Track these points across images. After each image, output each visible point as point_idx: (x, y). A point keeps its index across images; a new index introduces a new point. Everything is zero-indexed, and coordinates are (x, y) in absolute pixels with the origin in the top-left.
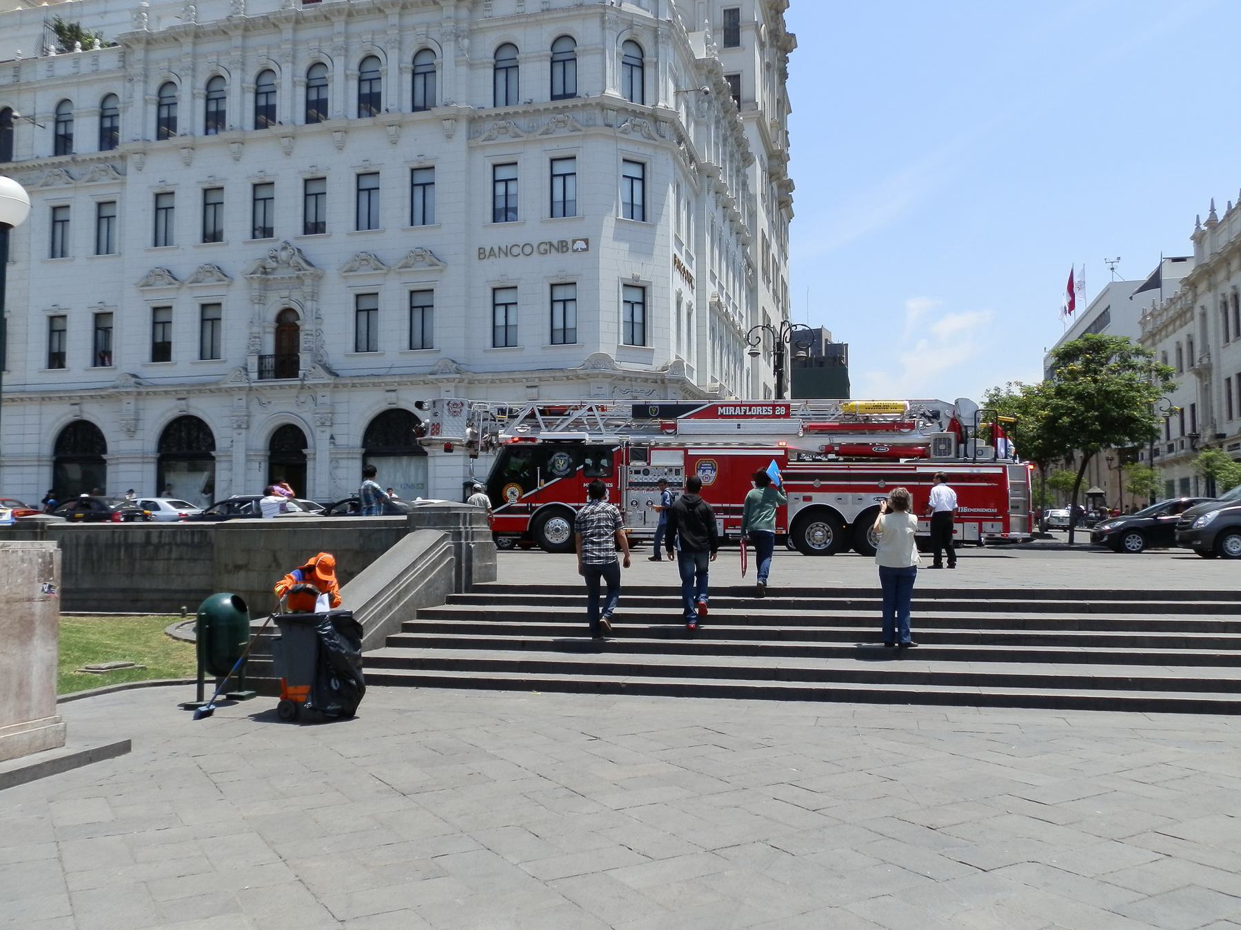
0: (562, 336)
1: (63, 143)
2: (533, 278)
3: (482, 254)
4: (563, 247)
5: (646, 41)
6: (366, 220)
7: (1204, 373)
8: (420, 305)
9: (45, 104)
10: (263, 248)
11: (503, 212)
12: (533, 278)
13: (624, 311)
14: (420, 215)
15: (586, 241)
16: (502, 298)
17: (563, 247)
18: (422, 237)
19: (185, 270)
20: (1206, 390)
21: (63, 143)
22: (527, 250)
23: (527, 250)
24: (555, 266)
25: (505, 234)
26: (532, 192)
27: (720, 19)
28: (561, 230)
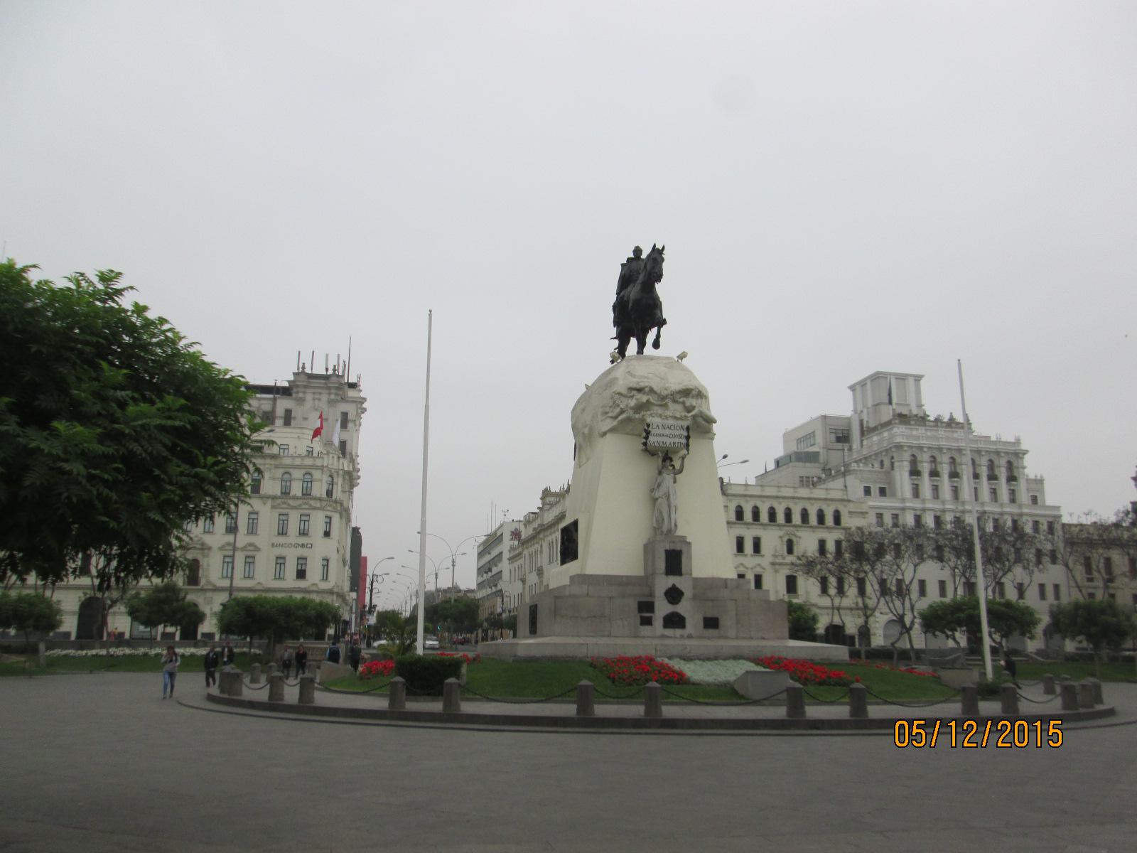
0: (301, 574)
3: (273, 545)
4: (303, 546)
5: (335, 474)
7: (523, 581)
8: (250, 561)
11: (282, 533)
13: (321, 568)
14: (252, 530)
15: (312, 545)
16: (280, 561)
17: (303, 546)
18: (252, 539)
20: (524, 588)
22: (290, 545)
23: (290, 545)
25: (282, 540)
26: (293, 526)
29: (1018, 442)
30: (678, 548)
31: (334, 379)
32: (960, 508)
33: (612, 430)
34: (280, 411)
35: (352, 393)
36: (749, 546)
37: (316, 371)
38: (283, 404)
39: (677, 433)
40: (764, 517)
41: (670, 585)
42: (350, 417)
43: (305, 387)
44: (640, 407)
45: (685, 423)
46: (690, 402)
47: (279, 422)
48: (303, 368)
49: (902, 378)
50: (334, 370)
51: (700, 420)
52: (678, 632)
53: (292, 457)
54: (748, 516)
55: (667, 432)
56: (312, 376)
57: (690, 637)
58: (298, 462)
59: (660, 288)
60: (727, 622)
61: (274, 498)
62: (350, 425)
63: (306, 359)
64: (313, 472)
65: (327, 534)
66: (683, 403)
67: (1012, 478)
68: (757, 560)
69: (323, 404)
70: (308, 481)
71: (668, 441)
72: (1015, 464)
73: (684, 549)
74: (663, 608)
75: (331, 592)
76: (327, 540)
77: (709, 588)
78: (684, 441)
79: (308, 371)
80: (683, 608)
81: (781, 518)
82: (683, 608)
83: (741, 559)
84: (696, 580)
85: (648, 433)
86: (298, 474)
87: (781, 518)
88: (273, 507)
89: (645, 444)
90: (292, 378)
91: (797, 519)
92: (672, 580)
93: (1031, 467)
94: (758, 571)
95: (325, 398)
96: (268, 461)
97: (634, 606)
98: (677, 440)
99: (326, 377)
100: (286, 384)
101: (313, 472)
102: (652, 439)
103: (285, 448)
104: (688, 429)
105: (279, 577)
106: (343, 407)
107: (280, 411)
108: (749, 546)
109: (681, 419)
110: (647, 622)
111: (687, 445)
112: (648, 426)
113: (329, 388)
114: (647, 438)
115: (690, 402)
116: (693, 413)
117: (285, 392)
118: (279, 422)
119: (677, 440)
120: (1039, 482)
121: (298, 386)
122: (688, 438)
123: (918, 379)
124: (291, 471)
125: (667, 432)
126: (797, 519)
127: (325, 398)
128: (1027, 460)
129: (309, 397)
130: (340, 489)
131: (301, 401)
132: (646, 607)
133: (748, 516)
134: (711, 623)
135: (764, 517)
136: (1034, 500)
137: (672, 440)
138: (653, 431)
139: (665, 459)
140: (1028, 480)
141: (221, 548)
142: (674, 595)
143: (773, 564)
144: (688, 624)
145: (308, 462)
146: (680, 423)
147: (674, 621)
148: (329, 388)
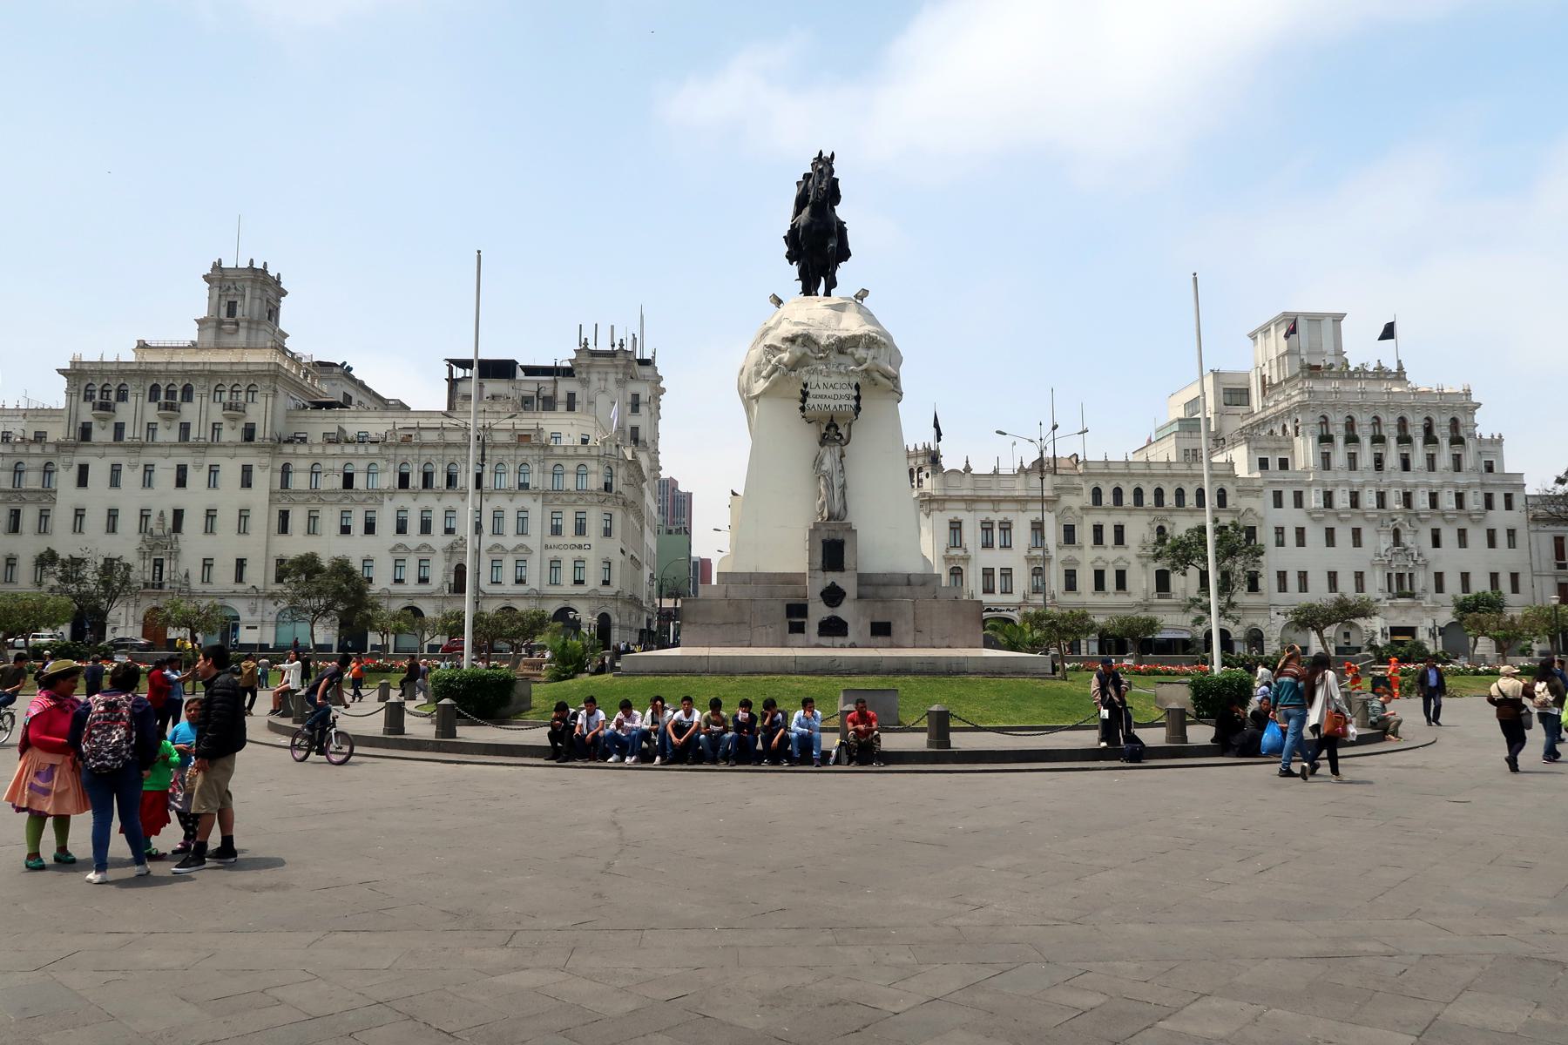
1: (348, 480)
2: (567, 558)
4: (580, 547)
6: (497, 532)
8: (520, 564)
9: (338, 465)
10: (450, 539)
11: (556, 531)
12: (567, 558)
14: (521, 531)
16: (555, 565)
17: (580, 547)
19: (412, 546)
21: (348, 480)
22: (566, 547)
23: (566, 547)
24: (577, 553)
25: (556, 540)
27: (629, 399)
28: (580, 540)
29: (1468, 393)
30: (840, 537)
31: (620, 355)
32: (1386, 481)
33: (764, 393)
34: (562, 396)
35: (646, 370)
36: (1109, 536)
37: (599, 348)
38: (565, 386)
39: (843, 392)
40: (1128, 499)
41: (829, 583)
42: (642, 398)
43: (589, 366)
44: (794, 366)
45: (854, 381)
46: (861, 353)
47: (562, 408)
48: (586, 344)
49: (1315, 319)
50: (621, 345)
51: (877, 375)
52: (839, 640)
53: (565, 447)
54: (1108, 498)
55: (831, 392)
56: (595, 354)
57: (853, 646)
58: (570, 452)
59: (841, 211)
60: (901, 627)
61: (545, 494)
62: (643, 409)
63: (588, 333)
64: (588, 463)
65: (608, 533)
66: (853, 355)
67: (1457, 440)
68: (1120, 552)
69: (612, 386)
70: (581, 472)
71: (832, 403)
72: (1462, 421)
73: (847, 539)
74: (819, 611)
75: (616, 597)
76: (607, 540)
77: (873, 587)
78: (853, 403)
79: (591, 347)
80: (845, 611)
81: (1149, 499)
82: (845, 611)
83: (1099, 552)
84: (864, 580)
85: (805, 395)
86: (570, 466)
87: (1149, 499)
88: (544, 504)
89: (803, 409)
90: (573, 356)
91: (1169, 500)
92: (832, 577)
93: (1485, 425)
94: (1121, 565)
95: (612, 377)
96: (536, 451)
97: (781, 610)
98: (843, 402)
99: (611, 354)
100: (568, 364)
101: (588, 463)
102: (810, 401)
103: (556, 436)
104: (857, 387)
105: (554, 583)
106: (634, 387)
107: (562, 396)
108: (1109, 536)
109: (847, 373)
110: (798, 628)
111: (858, 408)
112: (805, 385)
113: (616, 366)
114: (804, 401)
115: (861, 353)
116: (864, 366)
117: (568, 372)
118: (562, 408)
119: (843, 402)
120: (1497, 442)
121: (580, 365)
122: (858, 398)
123: (1338, 319)
124: (563, 462)
125: (831, 392)
126: (1169, 500)
127: (612, 377)
128: (1479, 416)
129: (594, 377)
130: (621, 481)
131: (585, 383)
132: (796, 614)
133: (1108, 498)
134: (881, 630)
135: (1128, 499)
136: (1490, 468)
137: (838, 403)
138: (812, 392)
139: (833, 432)
140: (1480, 441)
141: (490, 551)
142: (833, 596)
143: (1139, 557)
144: (850, 632)
145: (583, 451)
146: (846, 380)
147: (834, 628)
148: (616, 366)
